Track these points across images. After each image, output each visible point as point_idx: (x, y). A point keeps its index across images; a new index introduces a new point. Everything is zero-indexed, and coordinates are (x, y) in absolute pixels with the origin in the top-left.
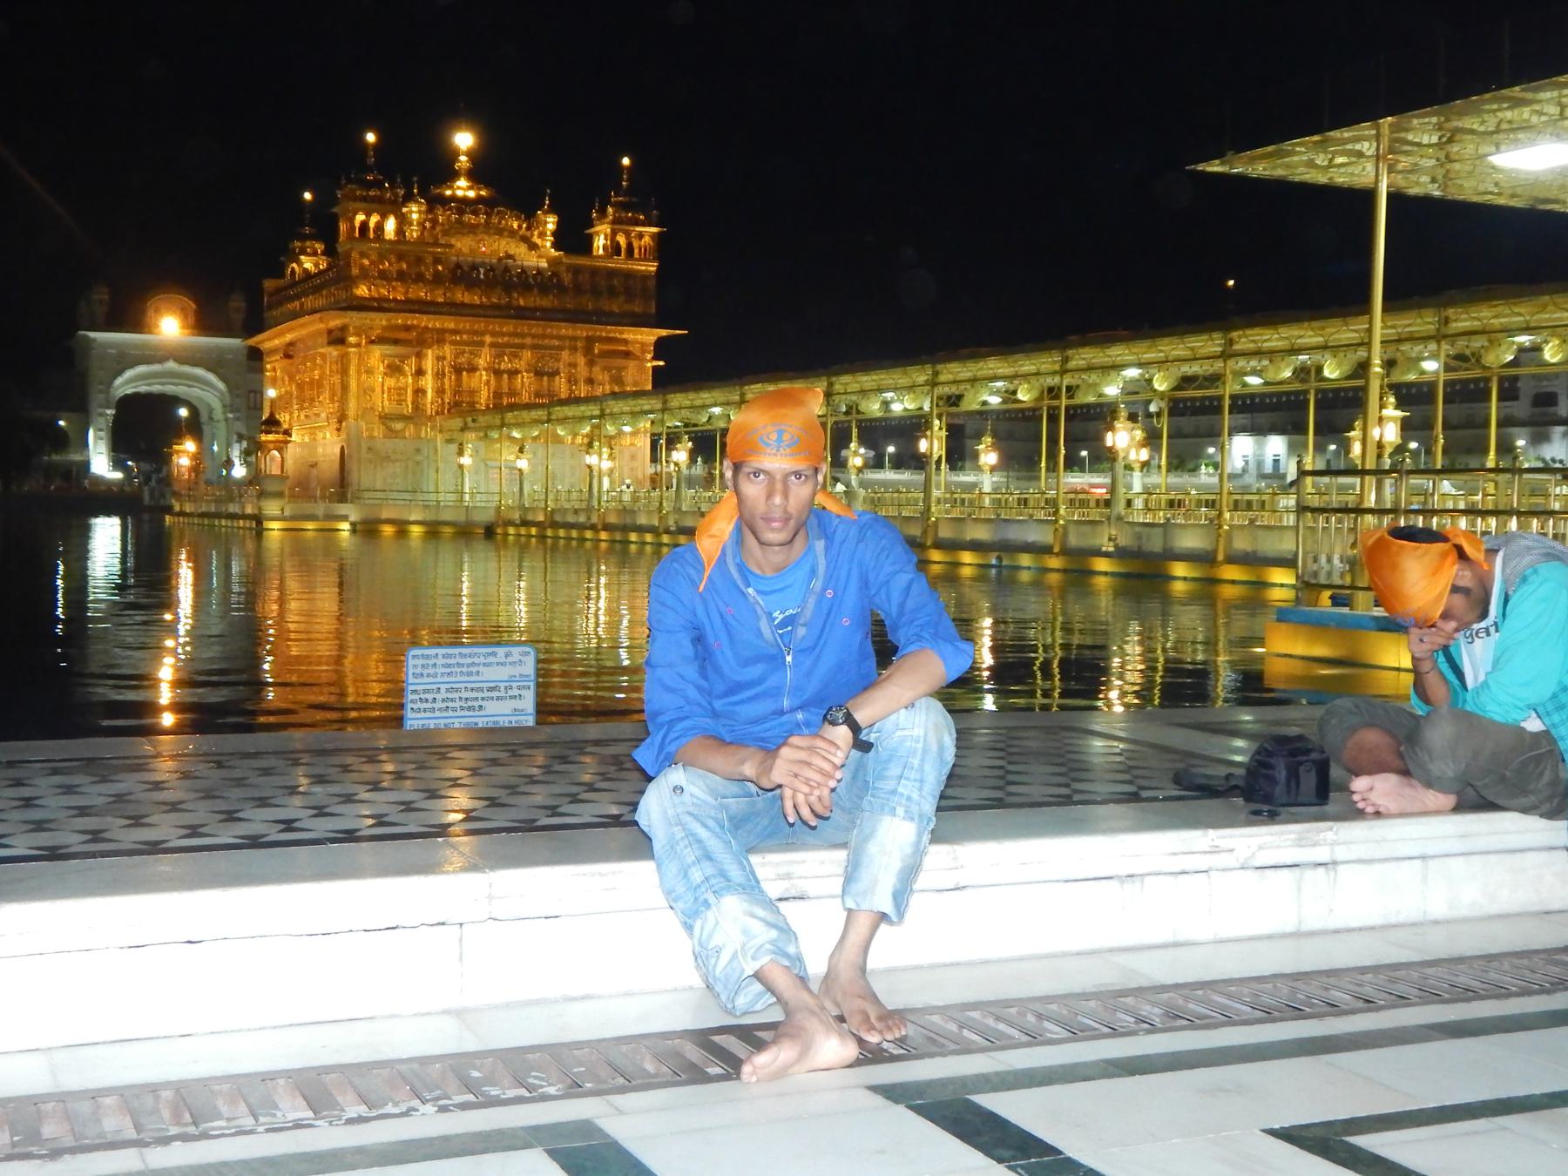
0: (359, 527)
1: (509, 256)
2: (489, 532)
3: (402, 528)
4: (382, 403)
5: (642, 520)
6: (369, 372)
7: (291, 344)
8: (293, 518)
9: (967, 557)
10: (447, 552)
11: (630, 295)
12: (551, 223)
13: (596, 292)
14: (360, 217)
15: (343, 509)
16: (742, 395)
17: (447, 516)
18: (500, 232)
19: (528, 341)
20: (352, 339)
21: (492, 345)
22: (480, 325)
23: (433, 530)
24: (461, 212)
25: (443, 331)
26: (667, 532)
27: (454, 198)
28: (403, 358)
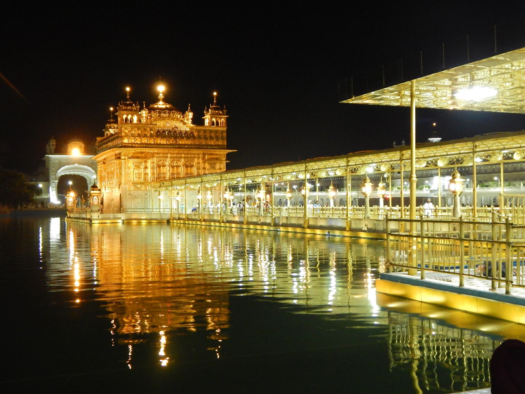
0: (125, 221)
1: (176, 127)
2: (168, 222)
3: (139, 220)
4: (133, 177)
5: (215, 218)
6: (129, 168)
7: (105, 159)
8: (102, 219)
9: (318, 232)
10: (155, 229)
11: (217, 138)
12: (190, 115)
13: (206, 138)
14: (124, 117)
15: (119, 215)
16: (245, 174)
17: (154, 217)
18: (173, 119)
19: (183, 155)
20: (123, 157)
21: (171, 157)
22: (166, 151)
23: (150, 222)
24: (160, 113)
26: (223, 222)
27: (158, 108)
28: (140, 163)
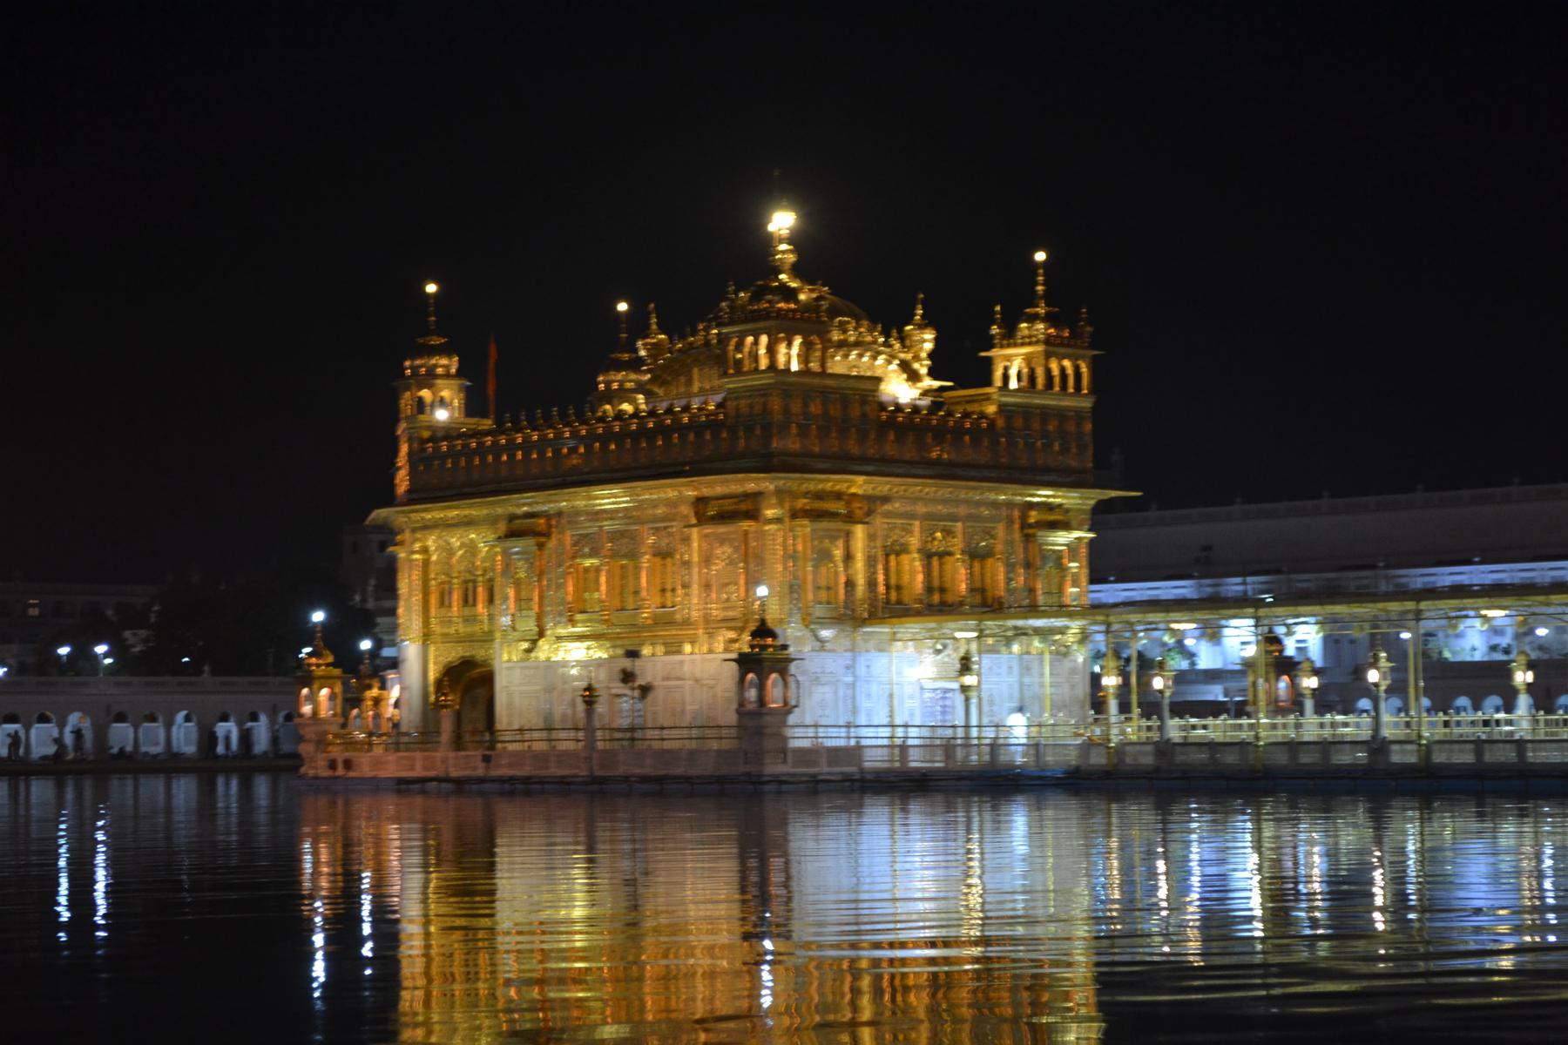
12: (927, 341)
19: (921, 509)
20: (770, 513)
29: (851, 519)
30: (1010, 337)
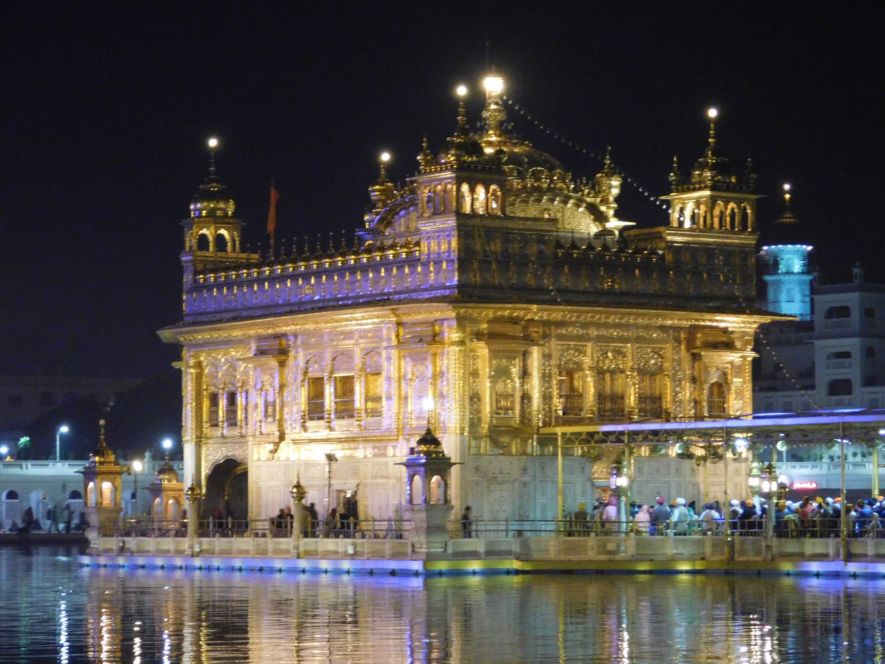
25: (546, 324)
29: (529, 340)
30: (686, 185)
